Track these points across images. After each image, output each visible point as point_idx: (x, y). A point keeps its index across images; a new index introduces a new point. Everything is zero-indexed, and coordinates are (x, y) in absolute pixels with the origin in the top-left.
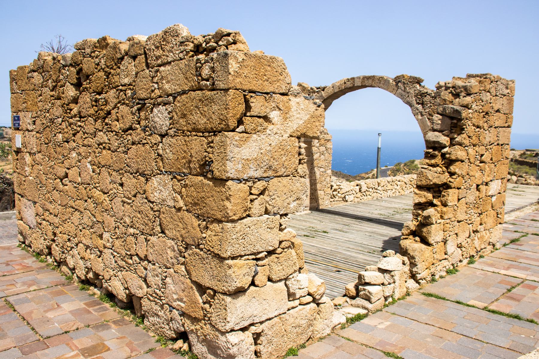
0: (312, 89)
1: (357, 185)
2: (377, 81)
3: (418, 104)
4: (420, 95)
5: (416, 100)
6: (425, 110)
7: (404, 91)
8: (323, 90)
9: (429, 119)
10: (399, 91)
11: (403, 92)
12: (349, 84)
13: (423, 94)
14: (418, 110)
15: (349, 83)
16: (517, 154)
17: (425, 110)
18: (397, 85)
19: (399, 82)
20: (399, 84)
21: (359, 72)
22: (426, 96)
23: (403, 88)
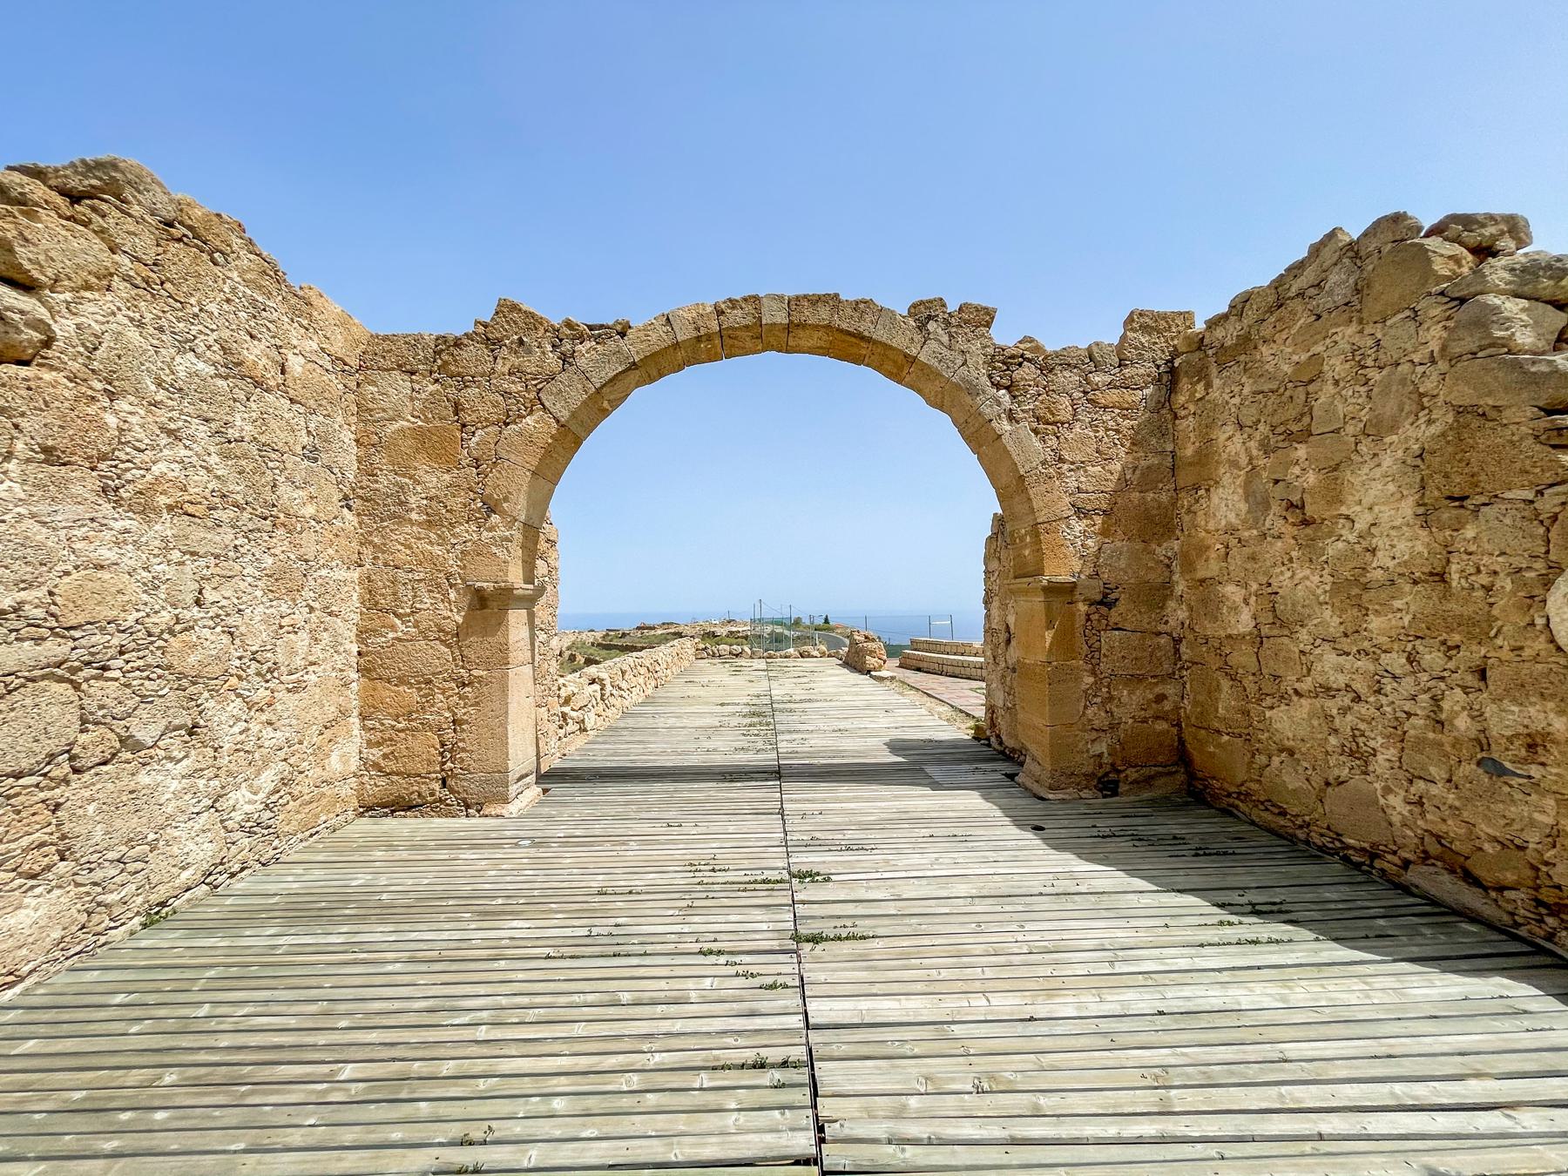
0: (569, 324)
1: (593, 682)
2: (849, 311)
3: (998, 386)
4: (1004, 363)
5: (990, 377)
6: (1019, 403)
7: (950, 348)
8: (623, 334)
9: (1036, 432)
10: (933, 345)
11: (945, 351)
12: (736, 318)
13: (1013, 357)
14: (999, 404)
15: (738, 312)
16: (599, 635)
17: (1019, 403)
18: (922, 327)
19: (929, 318)
20: (931, 326)
21: (780, 278)
22: (1020, 365)
23: (945, 339)
